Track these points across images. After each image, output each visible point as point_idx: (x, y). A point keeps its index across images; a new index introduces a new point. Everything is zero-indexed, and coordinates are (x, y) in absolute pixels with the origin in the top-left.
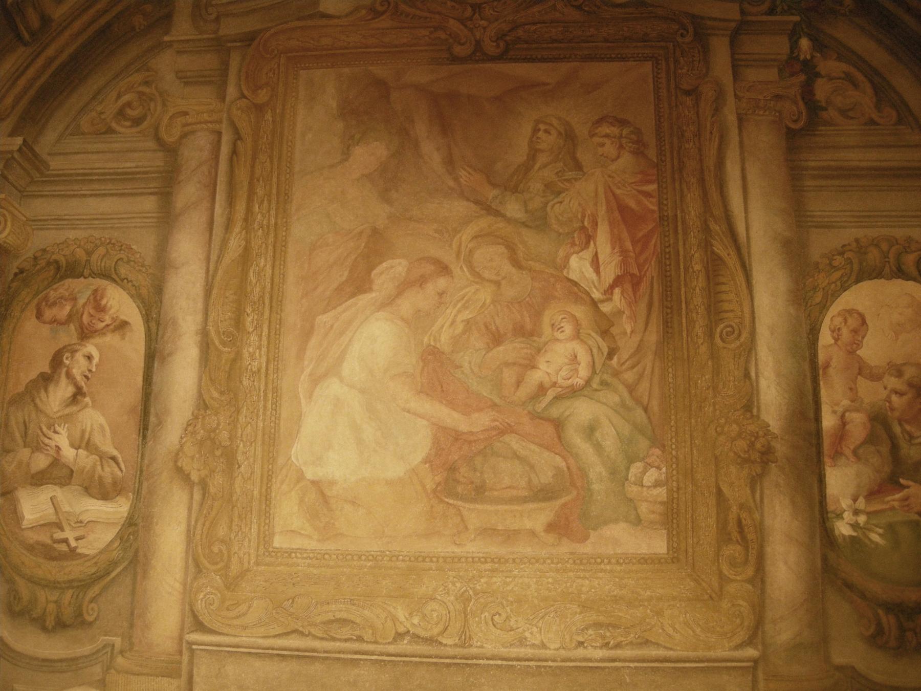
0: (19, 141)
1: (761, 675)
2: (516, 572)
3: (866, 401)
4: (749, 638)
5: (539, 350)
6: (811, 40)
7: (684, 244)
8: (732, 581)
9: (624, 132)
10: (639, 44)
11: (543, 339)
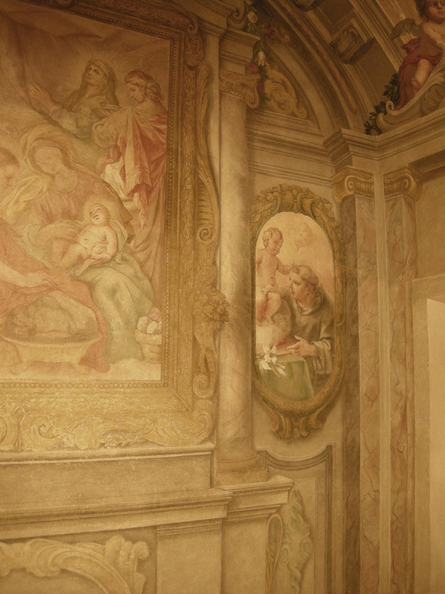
1: (215, 460)
2: (57, 394)
3: (280, 286)
4: (209, 436)
5: (80, 230)
6: (265, 54)
7: (182, 170)
8: (201, 398)
9: (149, 85)
10: (163, 27)
11: (83, 223)
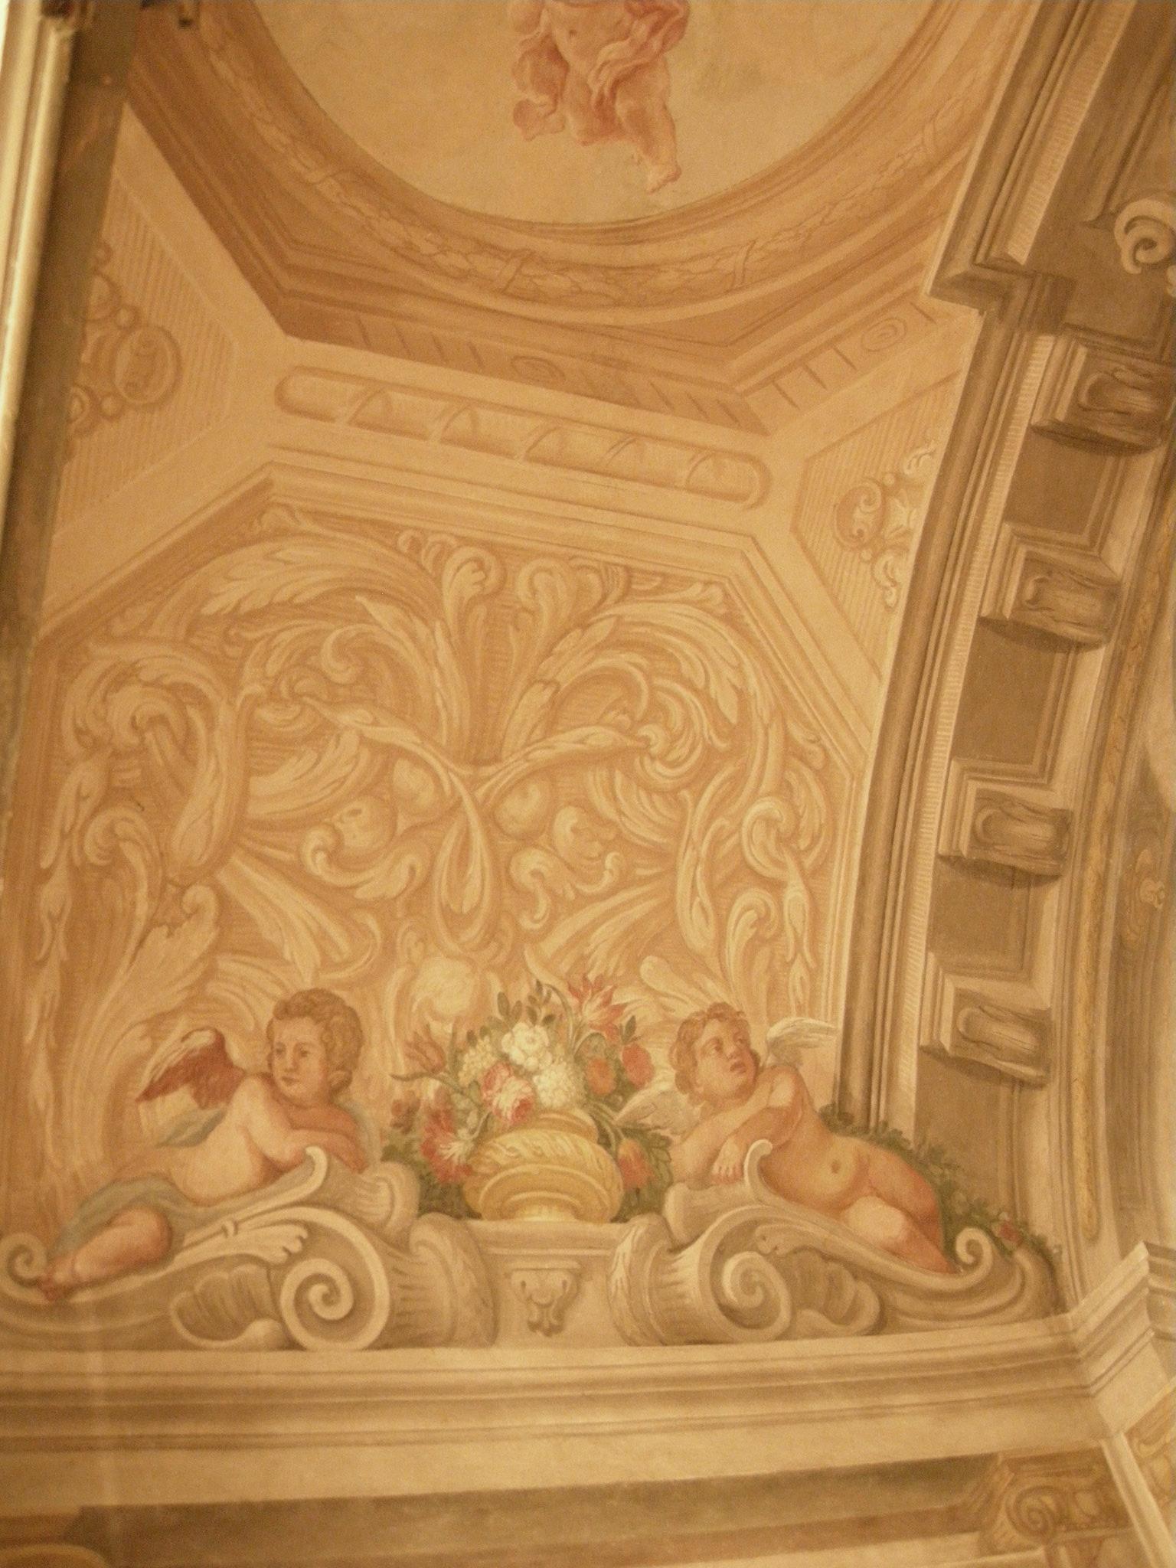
0: (1140, 1252)
